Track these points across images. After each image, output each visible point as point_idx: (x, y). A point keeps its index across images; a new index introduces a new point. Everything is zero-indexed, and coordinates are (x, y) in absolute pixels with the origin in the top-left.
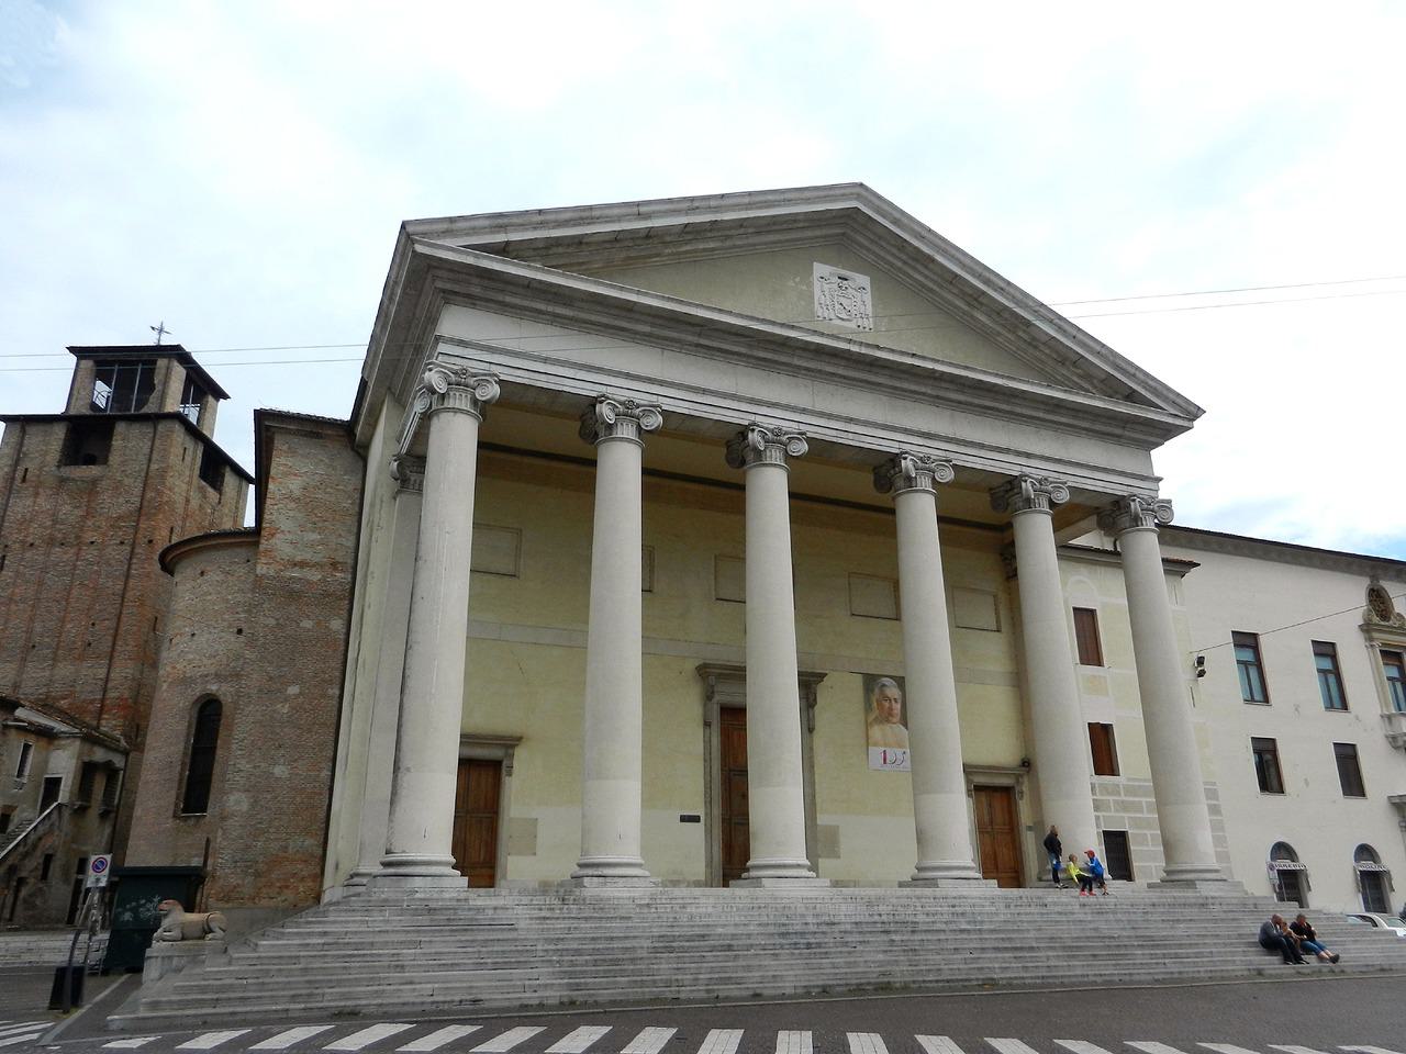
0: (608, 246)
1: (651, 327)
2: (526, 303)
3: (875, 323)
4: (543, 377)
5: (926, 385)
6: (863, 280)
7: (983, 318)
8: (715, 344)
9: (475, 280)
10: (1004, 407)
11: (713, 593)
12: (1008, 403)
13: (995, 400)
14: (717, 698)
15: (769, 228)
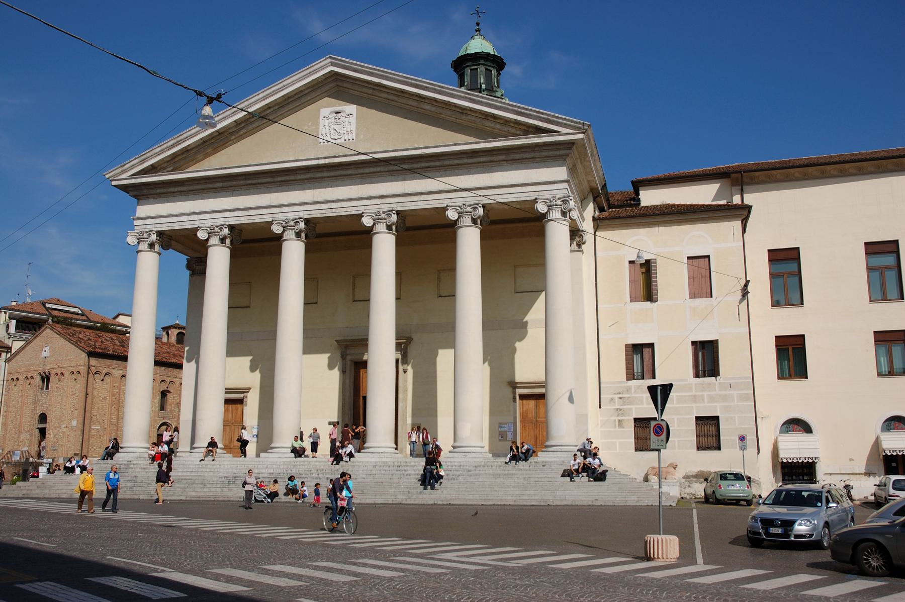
0: (202, 147)
1: (222, 182)
2: (165, 190)
3: (357, 135)
4: (177, 224)
5: (380, 166)
6: (352, 108)
7: (427, 107)
8: (254, 182)
9: (143, 187)
10: (437, 163)
11: (351, 298)
12: (439, 160)
13: (427, 161)
14: (349, 357)
15: (287, 102)
